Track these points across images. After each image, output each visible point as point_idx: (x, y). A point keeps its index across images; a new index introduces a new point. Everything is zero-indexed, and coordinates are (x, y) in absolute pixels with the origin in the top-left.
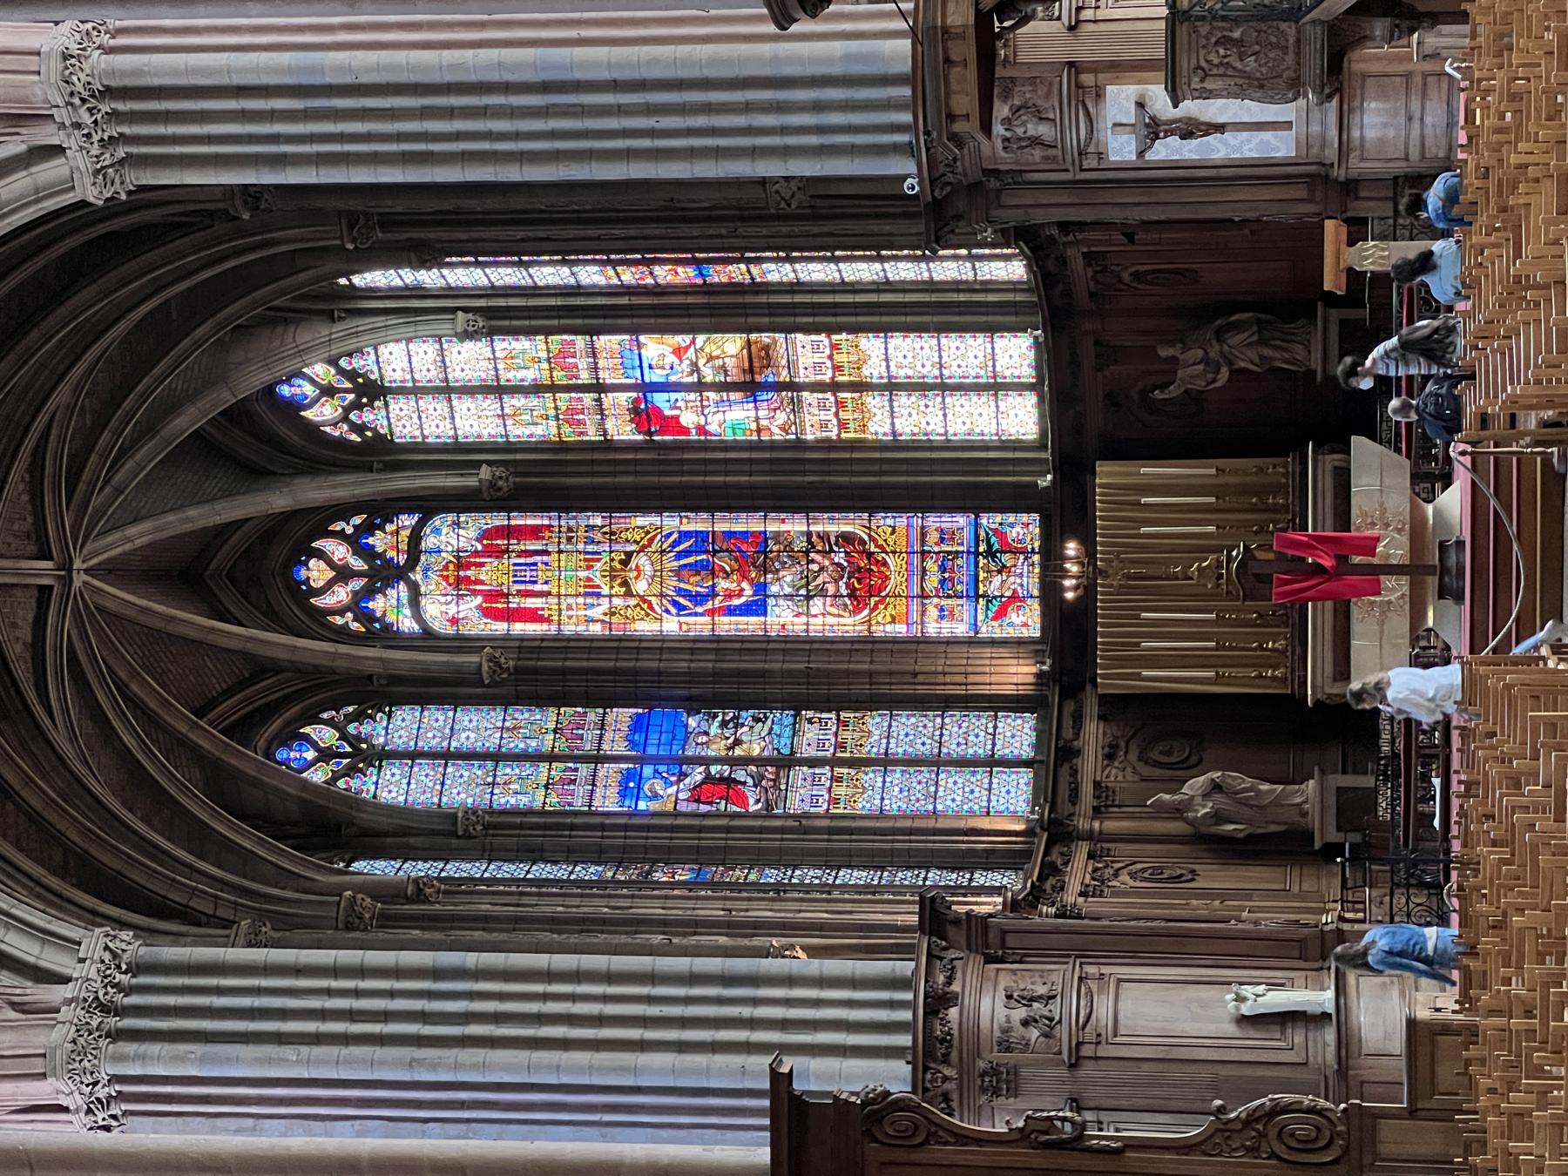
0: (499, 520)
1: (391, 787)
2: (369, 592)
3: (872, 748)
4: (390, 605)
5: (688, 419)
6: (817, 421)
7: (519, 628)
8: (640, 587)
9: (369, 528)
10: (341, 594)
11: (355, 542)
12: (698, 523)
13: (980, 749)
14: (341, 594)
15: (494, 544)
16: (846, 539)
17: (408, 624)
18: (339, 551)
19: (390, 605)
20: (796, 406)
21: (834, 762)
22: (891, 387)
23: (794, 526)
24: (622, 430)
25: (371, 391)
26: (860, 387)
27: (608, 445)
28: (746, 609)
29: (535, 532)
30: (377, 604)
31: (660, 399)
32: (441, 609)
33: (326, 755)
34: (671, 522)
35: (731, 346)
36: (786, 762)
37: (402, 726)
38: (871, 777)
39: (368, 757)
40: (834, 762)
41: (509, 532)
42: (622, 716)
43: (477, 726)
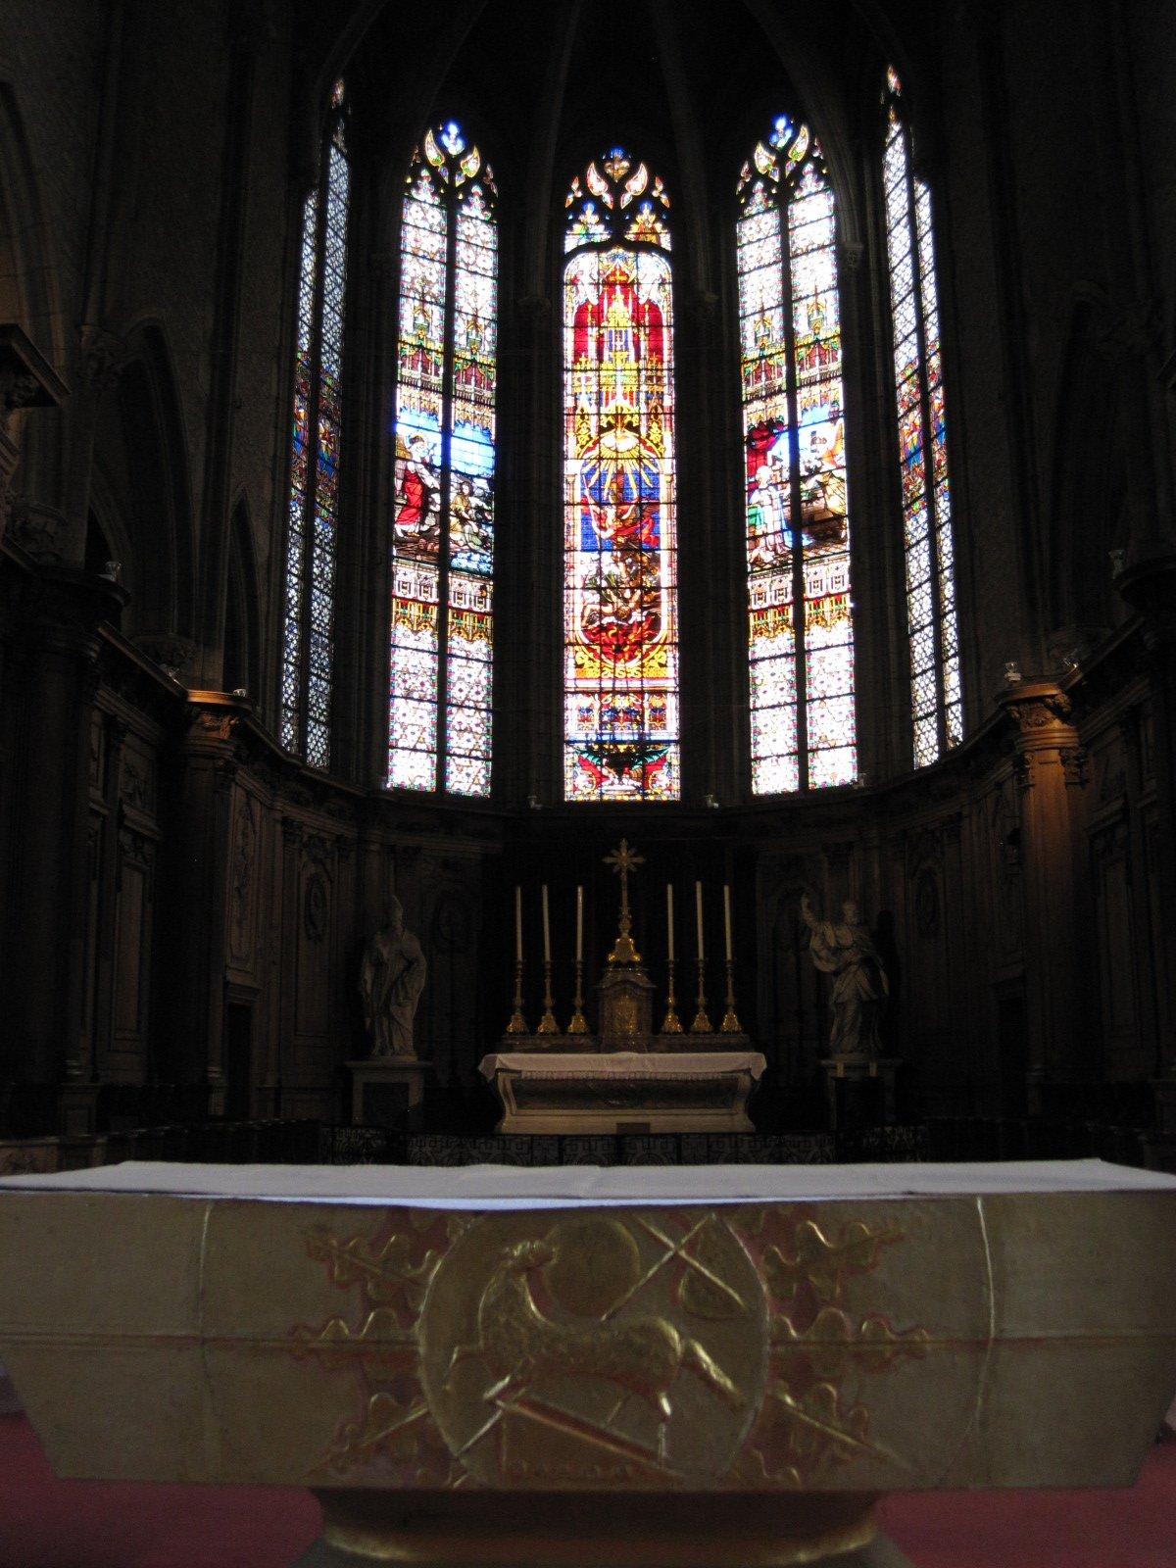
0: (667, 316)
1: (420, 218)
2: (600, 208)
3: (457, 643)
4: (592, 225)
5: (764, 474)
6: (767, 590)
7: (569, 336)
8: (608, 439)
9: (657, 208)
10: (598, 186)
11: (646, 195)
12: (666, 491)
13: (457, 742)
14: (598, 186)
15: (645, 317)
16: (654, 623)
17: (570, 244)
18: (637, 184)
19: (592, 225)
20: (778, 568)
21: (443, 605)
22: (800, 654)
23: (666, 575)
24: (753, 415)
25: (783, 196)
26: (799, 626)
27: (738, 406)
28: (588, 534)
29: (656, 349)
30: (590, 215)
31: (781, 447)
32: (584, 269)
33: (453, 163)
34: (667, 467)
35: (836, 501)
36: (443, 562)
37: (478, 230)
38: (427, 639)
39: (451, 201)
40: (443, 605)
41: (656, 326)
42: (490, 418)
43: (478, 294)
